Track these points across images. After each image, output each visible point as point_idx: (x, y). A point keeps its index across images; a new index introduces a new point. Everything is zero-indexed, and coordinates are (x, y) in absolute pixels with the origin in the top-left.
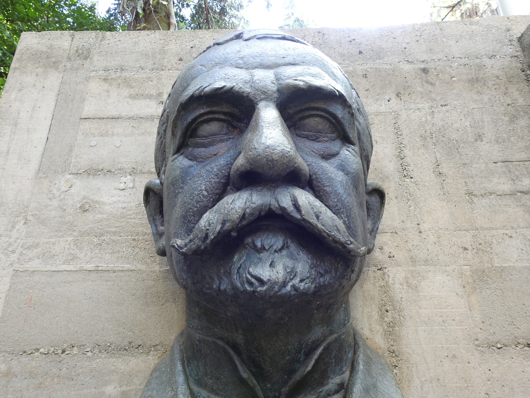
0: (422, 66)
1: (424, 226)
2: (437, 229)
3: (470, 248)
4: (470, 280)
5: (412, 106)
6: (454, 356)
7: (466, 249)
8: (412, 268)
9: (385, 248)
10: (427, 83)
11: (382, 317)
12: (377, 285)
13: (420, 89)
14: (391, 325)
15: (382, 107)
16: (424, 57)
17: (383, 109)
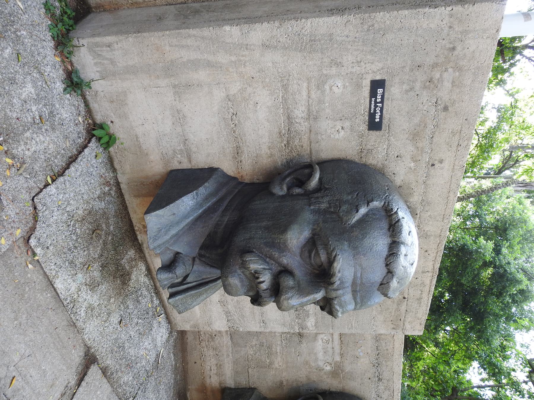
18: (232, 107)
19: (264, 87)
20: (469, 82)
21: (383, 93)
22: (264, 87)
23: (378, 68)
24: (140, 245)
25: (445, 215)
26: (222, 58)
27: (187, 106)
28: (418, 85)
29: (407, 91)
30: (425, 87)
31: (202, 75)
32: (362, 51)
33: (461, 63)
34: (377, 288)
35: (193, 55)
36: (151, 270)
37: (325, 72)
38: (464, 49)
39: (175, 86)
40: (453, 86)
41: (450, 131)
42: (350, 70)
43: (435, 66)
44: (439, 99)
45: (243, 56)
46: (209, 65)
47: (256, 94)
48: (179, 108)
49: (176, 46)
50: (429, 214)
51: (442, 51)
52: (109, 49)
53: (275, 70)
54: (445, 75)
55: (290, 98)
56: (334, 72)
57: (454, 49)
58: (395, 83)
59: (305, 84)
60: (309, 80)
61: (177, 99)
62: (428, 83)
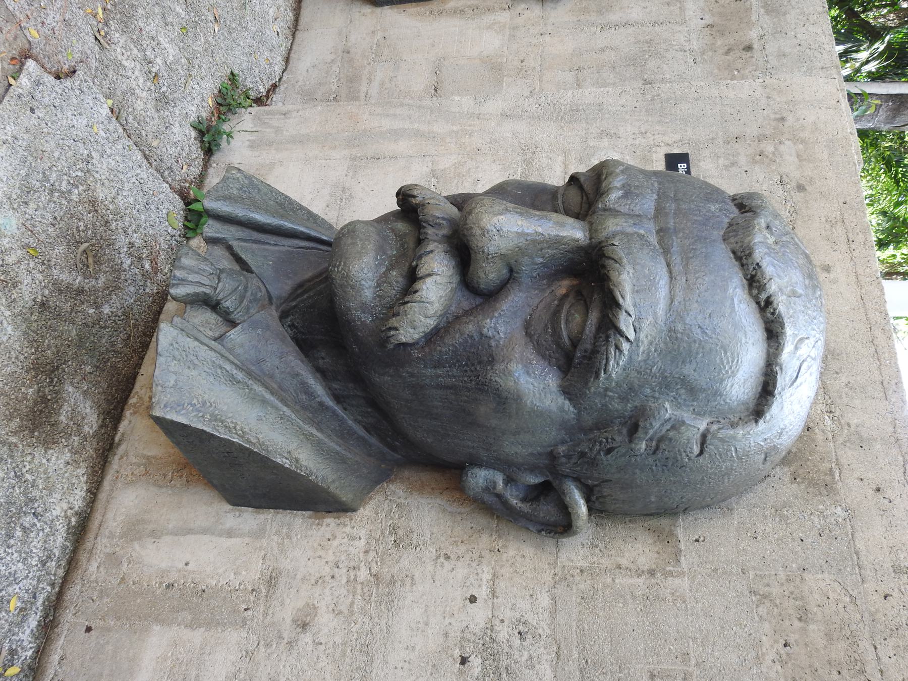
0: (755, 46)
1: (547, 38)
2: (544, 45)
3: (523, 64)
4: (493, 61)
5: (693, 36)
6: (433, 46)
7: (522, 61)
8: (507, 26)
9: (529, 11)
10: (729, 50)
11: (469, 7)
12: (496, 5)
13: (719, 43)
14: (462, 11)
15: (692, 13)
16: (771, 48)
17: (689, 13)
18: (436, 184)
19: (494, 161)
20: (825, 155)
21: (688, 167)
22: (494, 161)
23: (674, 140)
24: (112, 444)
25: (885, 383)
26: (440, 128)
27: (362, 184)
28: (742, 160)
29: (726, 167)
30: (754, 162)
31: (403, 146)
32: (647, 121)
33: (802, 135)
34: (722, 233)
35: (398, 124)
36: (85, 533)
37: (592, 144)
38: (798, 120)
39: (354, 159)
40: (800, 161)
41: (823, 219)
42: (631, 141)
43: (761, 138)
44: (784, 176)
45: (470, 126)
46: (418, 134)
47: (479, 169)
48: (347, 185)
49: (378, 114)
50: (844, 379)
51: (767, 122)
52: (283, 117)
53: (515, 141)
54: (782, 148)
55: (534, 174)
56: (606, 144)
57: (783, 119)
58: (705, 157)
59: (560, 159)
60: (566, 153)
61: (351, 174)
62: (758, 157)
